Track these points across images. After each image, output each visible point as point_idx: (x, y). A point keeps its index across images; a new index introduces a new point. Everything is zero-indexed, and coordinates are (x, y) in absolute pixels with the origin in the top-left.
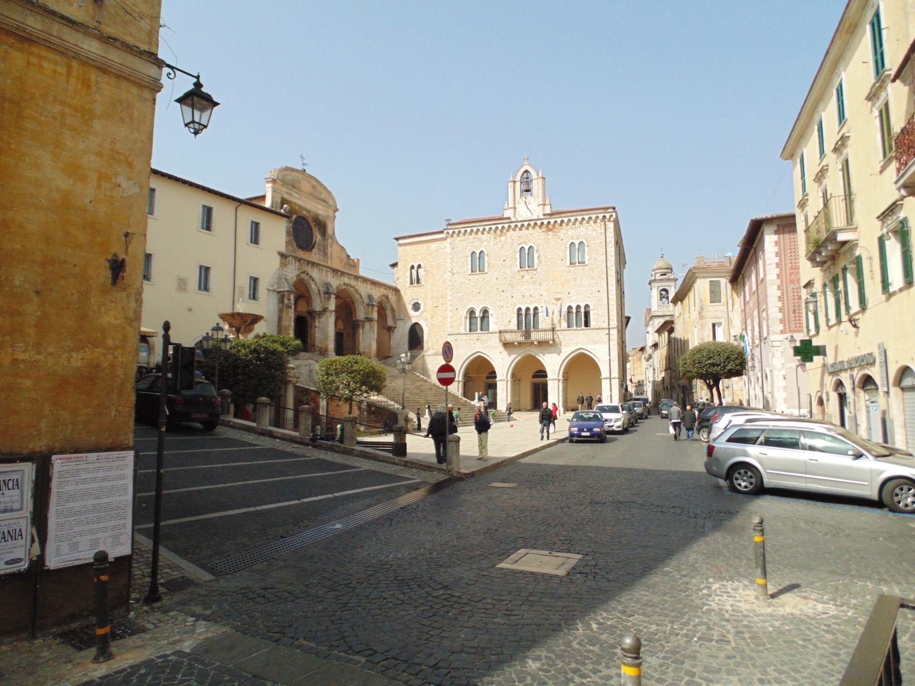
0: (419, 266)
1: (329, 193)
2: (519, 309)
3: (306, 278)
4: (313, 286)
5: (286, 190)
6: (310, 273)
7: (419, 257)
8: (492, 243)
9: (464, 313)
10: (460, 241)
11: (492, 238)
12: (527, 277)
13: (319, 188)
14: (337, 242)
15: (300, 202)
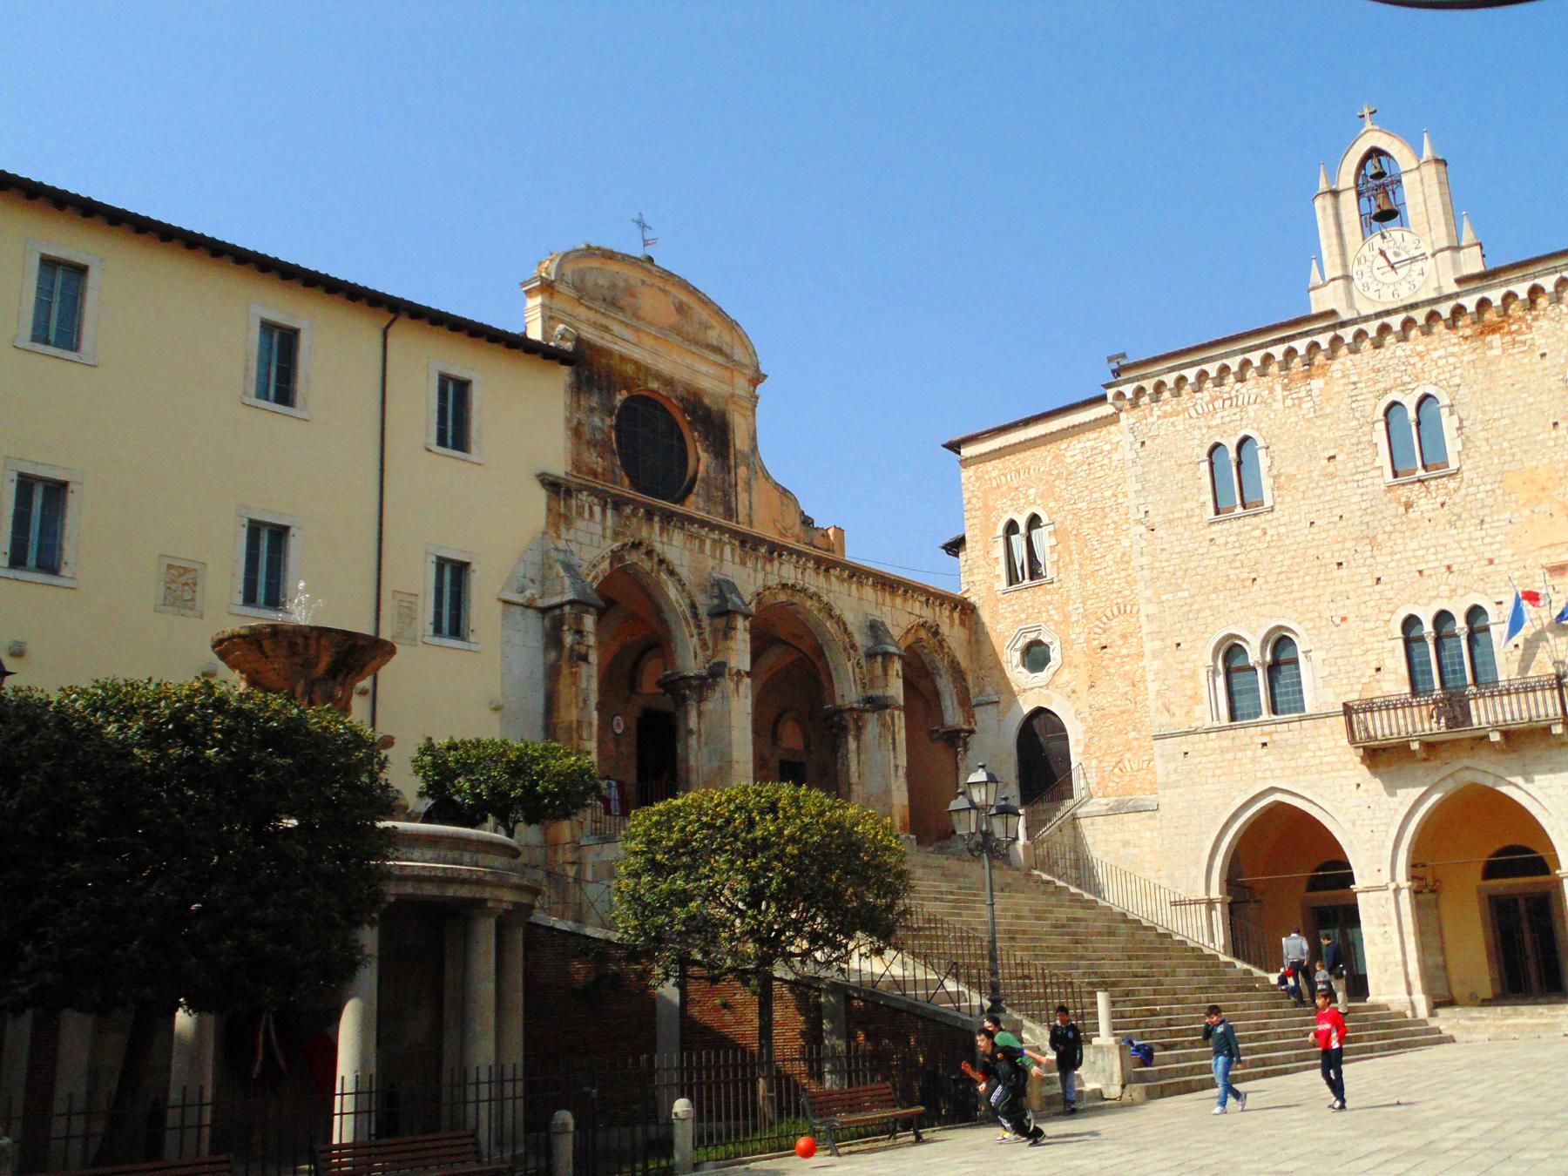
0: (1034, 521)
1: (733, 326)
2: (1411, 622)
3: (647, 565)
4: (673, 593)
5: (591, 315)
6: (658, 547)
7: (1032, 492)
8: (1278, 405)
9: (1203, 656)
10: (1166, 415)
11: (1278, 388)
12: (1425, 504)
13: (701, 313)
14: (768, 477)
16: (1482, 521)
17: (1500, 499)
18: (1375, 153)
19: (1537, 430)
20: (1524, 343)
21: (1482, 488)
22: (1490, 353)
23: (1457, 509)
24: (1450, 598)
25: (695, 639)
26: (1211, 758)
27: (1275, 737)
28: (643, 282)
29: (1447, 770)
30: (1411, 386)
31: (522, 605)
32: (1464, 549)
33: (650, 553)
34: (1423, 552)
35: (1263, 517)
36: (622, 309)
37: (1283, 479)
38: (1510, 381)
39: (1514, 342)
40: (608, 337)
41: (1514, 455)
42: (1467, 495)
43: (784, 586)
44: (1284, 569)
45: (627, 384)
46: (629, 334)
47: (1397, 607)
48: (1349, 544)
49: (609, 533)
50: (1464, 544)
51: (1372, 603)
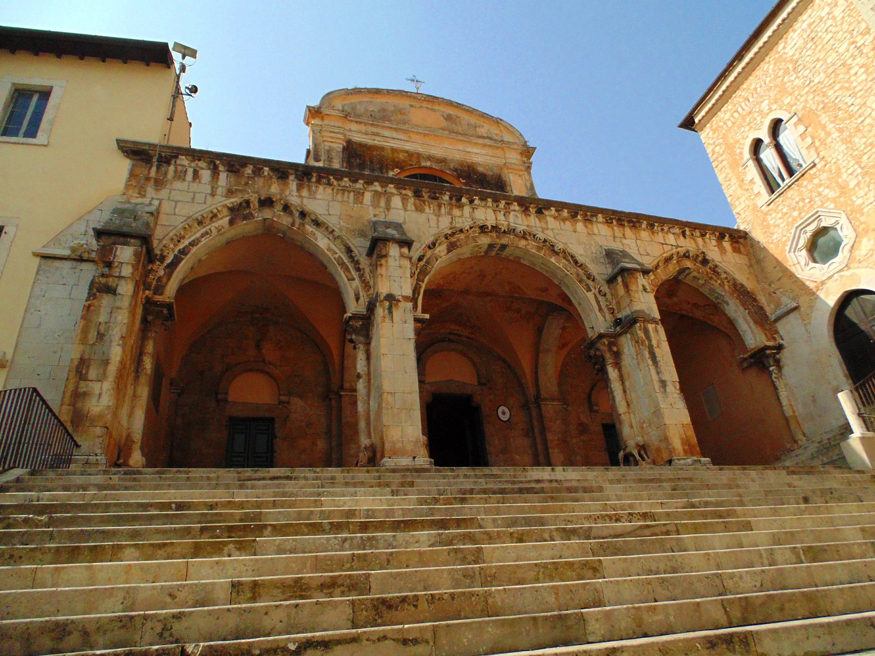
0: (776, 126)
1: (497, 122)
4: (322, 242)
7: (765, 106)
13: (465, 117)
15: (409, 147)
25: (357, 283)
28: (412, 106)
33: (286, 208)
43: (483, 229)
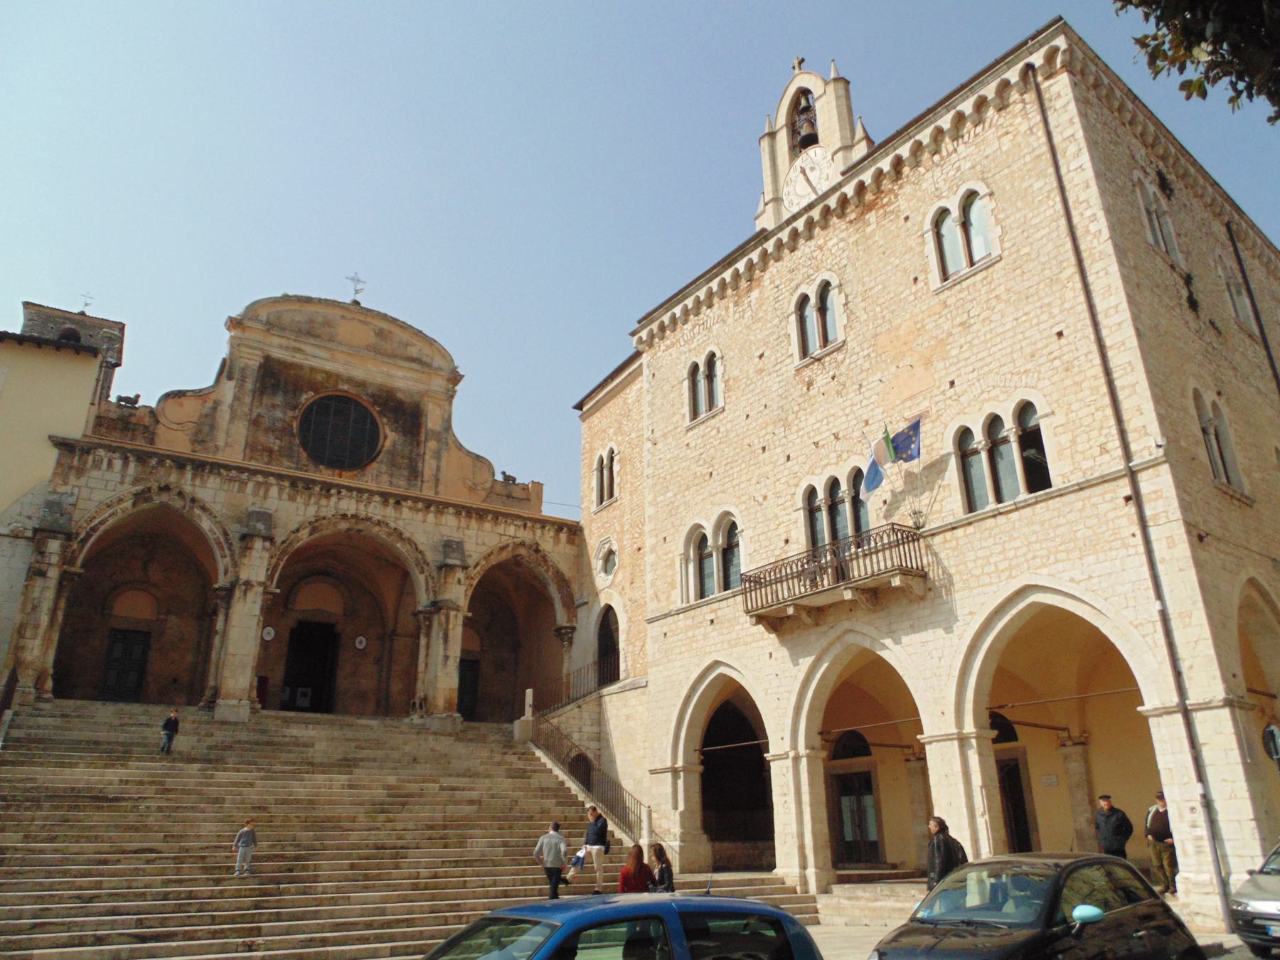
1: (431, 342)
2: (811, 493)
3: (178, 503)
4: (206, 524)
5: (284, 342)
6: (188, 488)
8: (730, 321)
9: (677, 546)
10: (668, 347)
11: (731, 305)
12: (821, 379)
14: (460, 447)
15: (329, 366)
16: (861, 385)
17: (873, 361)
18: (805, 92)
19: (901, 289)
20: (892, 212)
21: (861, 354)
22: (869, 230)
23: (843, 379)
24: (837, 464)
25: (228, 560)
26: (680, 636)
27: (719, 613)
28: (343, 317)
29: (833, 634)
30: (813, 277)
31: (8, 536)
32: (847, 415)
33: (181, 494)
34: (819, 425)
35: (717, 418)
36: (318, 336)
37: (731, 382)
38: (882, 250)
39: (886, 213)
40: (298, 355)
41: (884, 317)
42: (850, 364)
43: (344, 516)
44: (729, 460)
45: (314, 387)
46: (324, 354)
47: (800, 479)
48: (770, 429)
49: (128, 479)
50: (847, 411)
51: (783, 480)
